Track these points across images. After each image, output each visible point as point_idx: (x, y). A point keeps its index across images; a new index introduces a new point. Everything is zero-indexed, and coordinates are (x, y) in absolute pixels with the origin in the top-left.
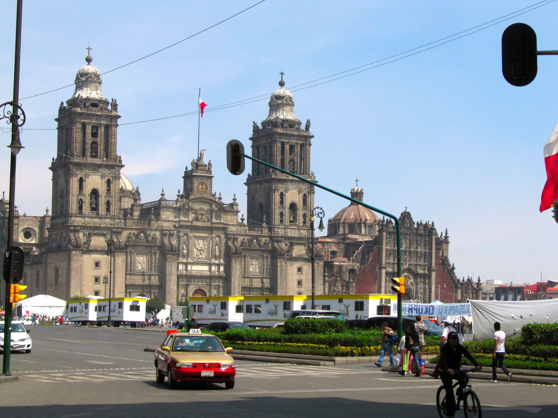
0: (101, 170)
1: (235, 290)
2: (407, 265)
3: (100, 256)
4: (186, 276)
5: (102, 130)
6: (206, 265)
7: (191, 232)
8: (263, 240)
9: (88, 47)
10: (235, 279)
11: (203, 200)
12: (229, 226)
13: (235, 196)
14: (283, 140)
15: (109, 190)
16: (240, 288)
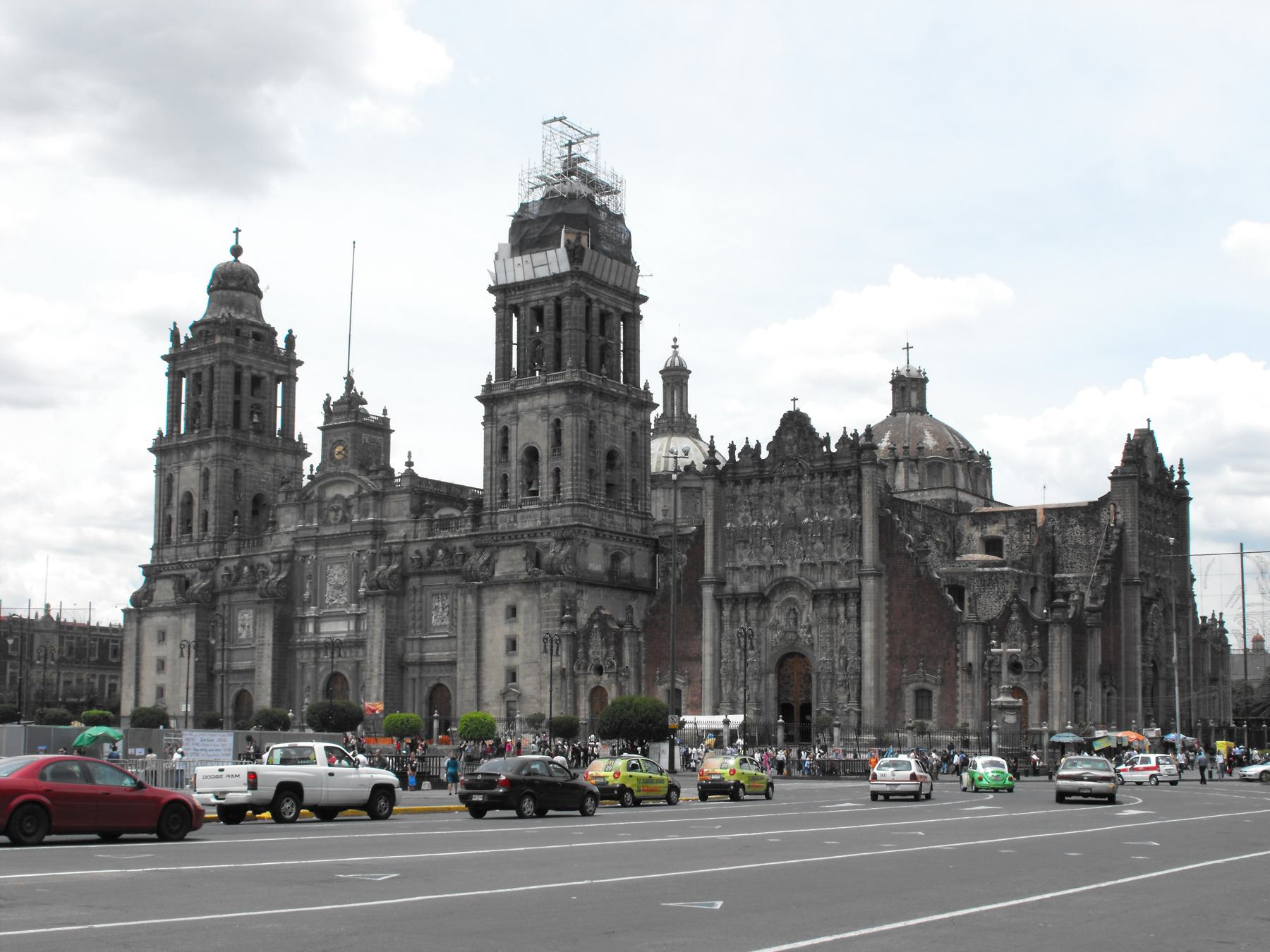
0: (195, 454)
1: (371, 671)
2: (798, 568)
3: (165, 618)
4: (304, 647)
5: (206, 376)
6: (346, 620)
7: (316, 552)
8: (458, 544)
9: (235, 230)
10: (372, 646)
11: (337, 478)
12: (391, 526)
13: (410, 455)
14: (514, 302)
15: (206, 489)
16: (383, 666)
